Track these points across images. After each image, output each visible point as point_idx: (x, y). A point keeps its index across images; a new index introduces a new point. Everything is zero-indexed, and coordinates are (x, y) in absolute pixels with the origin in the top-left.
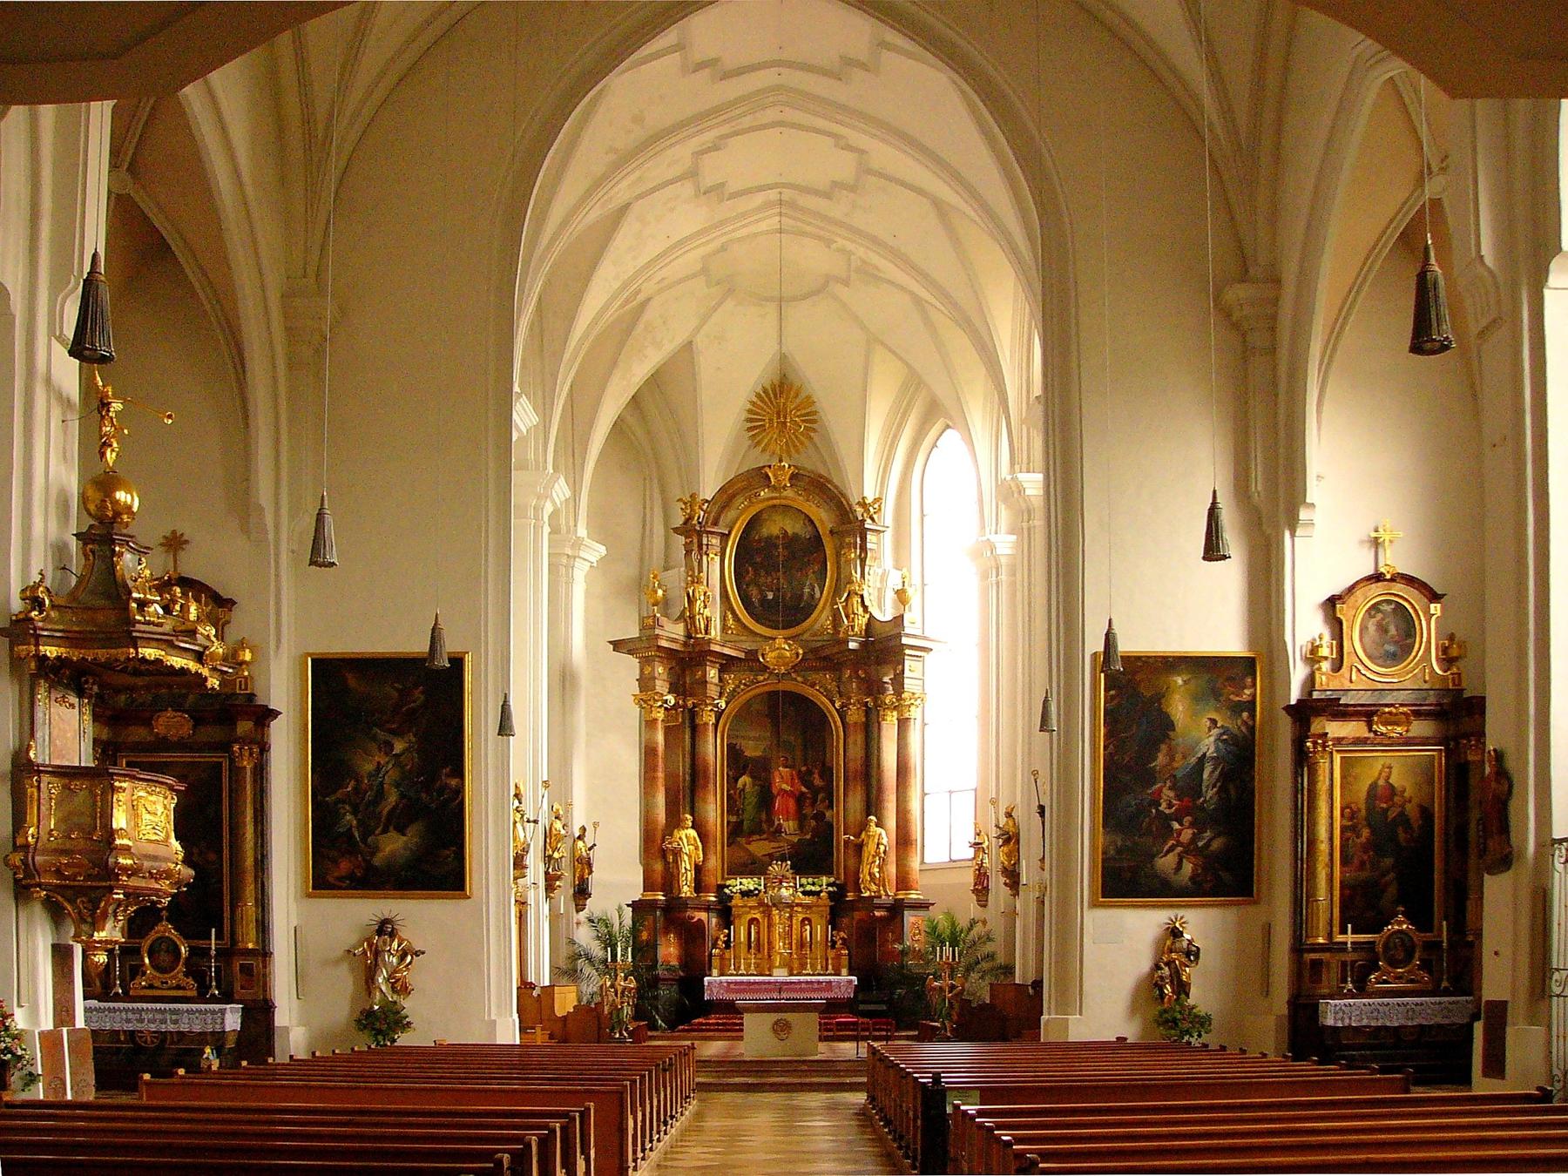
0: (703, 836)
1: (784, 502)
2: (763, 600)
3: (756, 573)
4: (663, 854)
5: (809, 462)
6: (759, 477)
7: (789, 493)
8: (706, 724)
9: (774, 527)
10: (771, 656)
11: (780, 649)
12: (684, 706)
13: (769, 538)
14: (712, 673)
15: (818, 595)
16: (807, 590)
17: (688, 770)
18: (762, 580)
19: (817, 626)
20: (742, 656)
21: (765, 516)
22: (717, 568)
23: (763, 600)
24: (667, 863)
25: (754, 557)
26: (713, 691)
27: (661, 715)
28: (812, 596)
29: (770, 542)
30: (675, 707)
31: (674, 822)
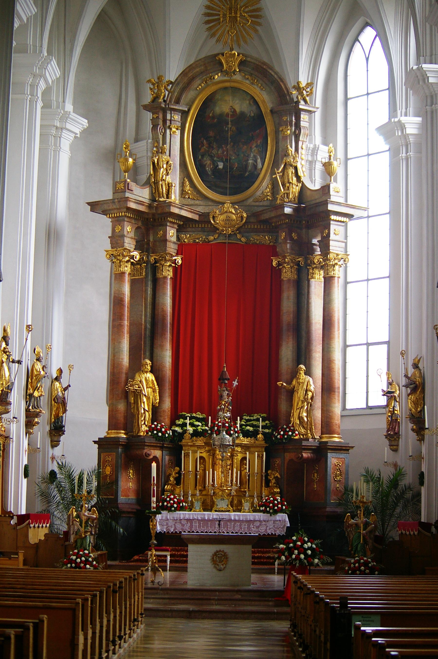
0: (159, 380)
1: (233, 84)
2: (215, 169)
3: (210, 146)
4: (126, 394)
5: (255, 52)
6: (213, 63)
7: (238, 77)
8: (165, 278)
9: (226, 106)
10: (220, 219)
11: (228, 213)
12: (147, 262)
13: (221, 115)
14: (171, 233)
15: (260, 166)
16: (250, 161)
17: (149, 319)
18: (214, 152)
19: (259, 193)
20: (196, 217)
21: (218, 96)
22: (177, 142)
23: (215, 169)
24: (128, 404)
25: (207, 132)
26: (172, 248)
27: (127, 269)
28: (255, 166)
29: (221, 119)
30: (139, 263)
31: (136, 367)
